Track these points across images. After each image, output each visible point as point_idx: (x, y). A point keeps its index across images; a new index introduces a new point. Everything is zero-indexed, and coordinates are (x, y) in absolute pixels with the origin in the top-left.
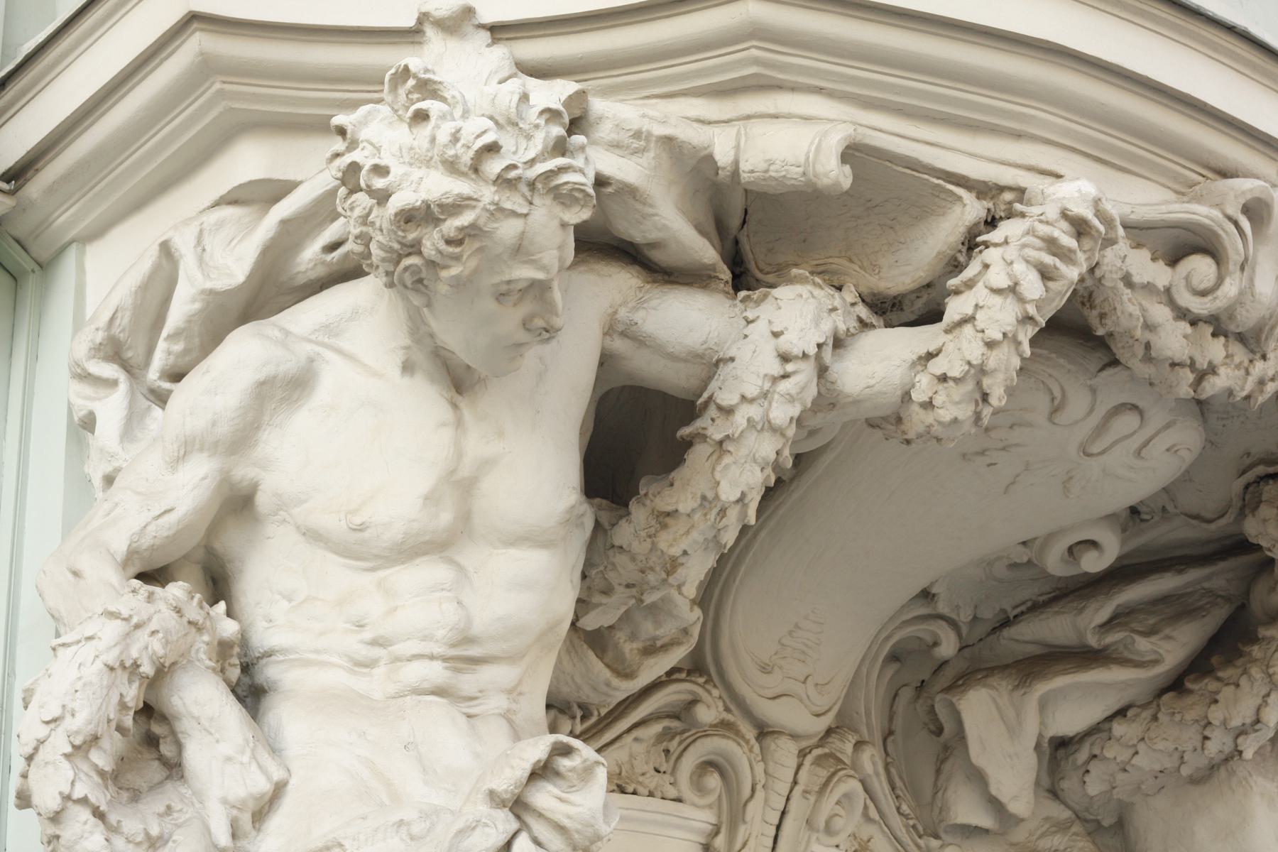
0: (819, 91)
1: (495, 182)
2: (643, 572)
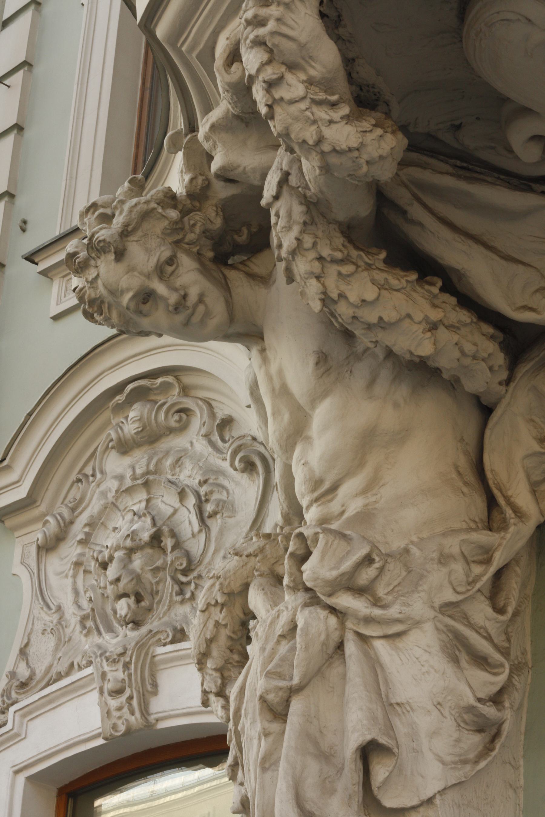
0: (216, 34)
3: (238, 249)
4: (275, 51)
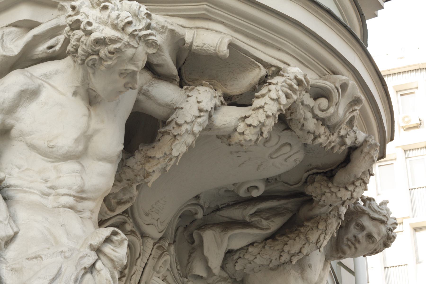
0: (222, 23)
1: (129, 35)
2: (136, 176)
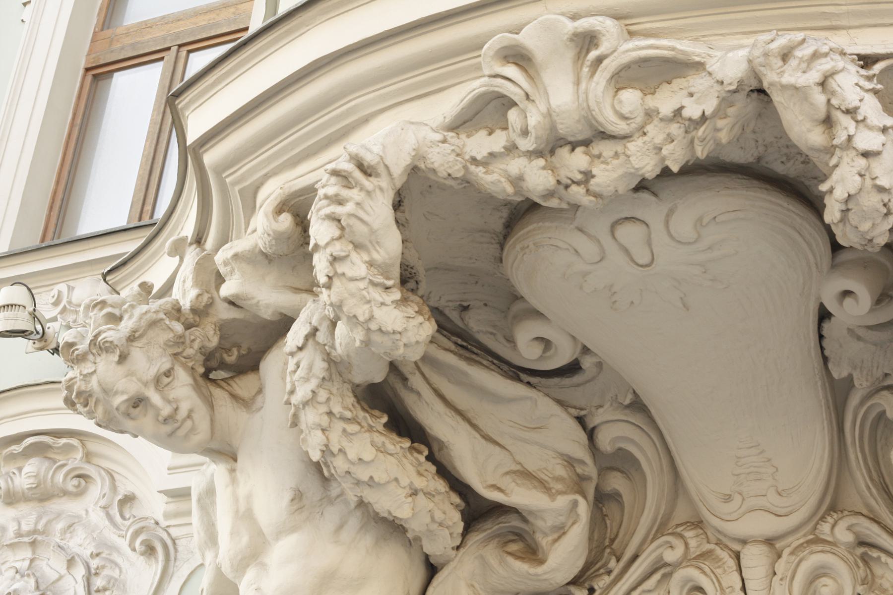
0: (266, 177)
3: (223, 366)
4: (347, 230)
